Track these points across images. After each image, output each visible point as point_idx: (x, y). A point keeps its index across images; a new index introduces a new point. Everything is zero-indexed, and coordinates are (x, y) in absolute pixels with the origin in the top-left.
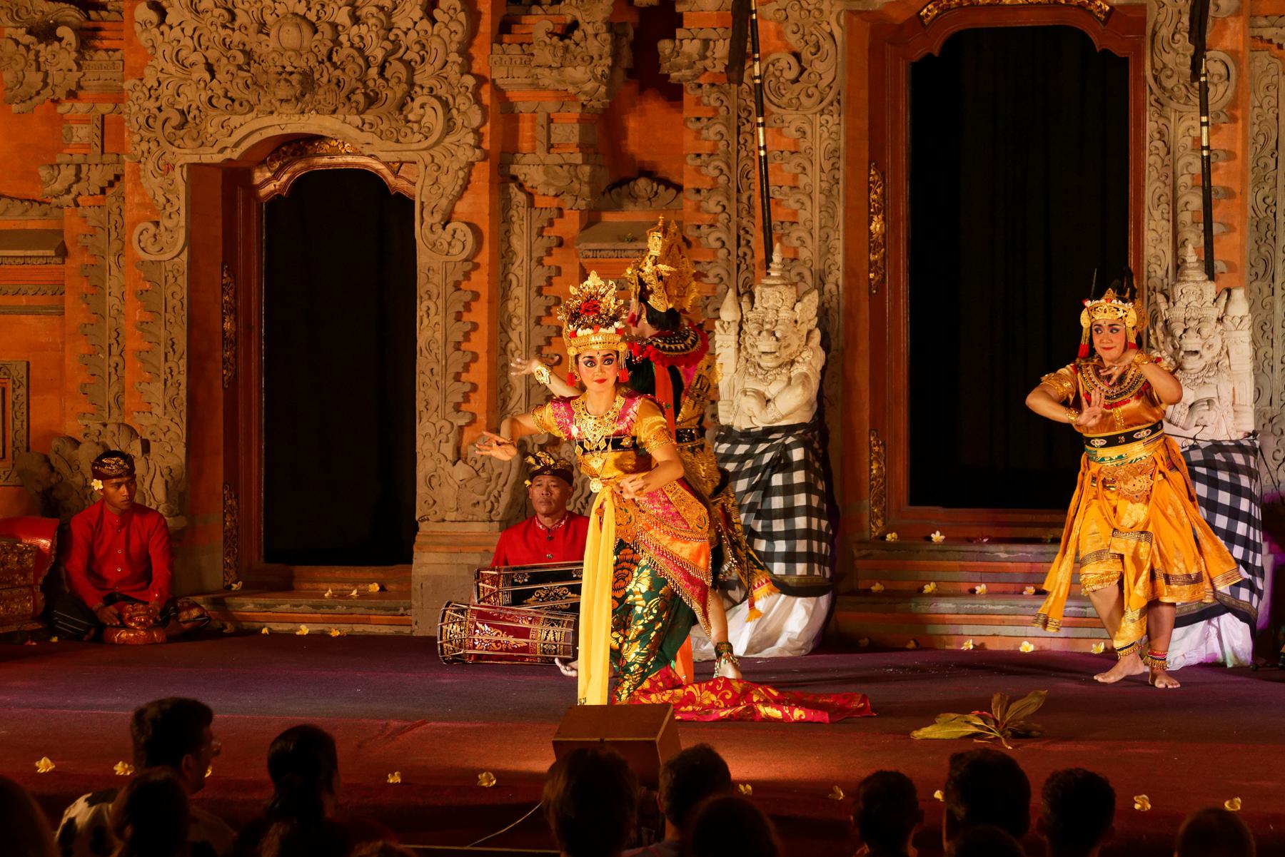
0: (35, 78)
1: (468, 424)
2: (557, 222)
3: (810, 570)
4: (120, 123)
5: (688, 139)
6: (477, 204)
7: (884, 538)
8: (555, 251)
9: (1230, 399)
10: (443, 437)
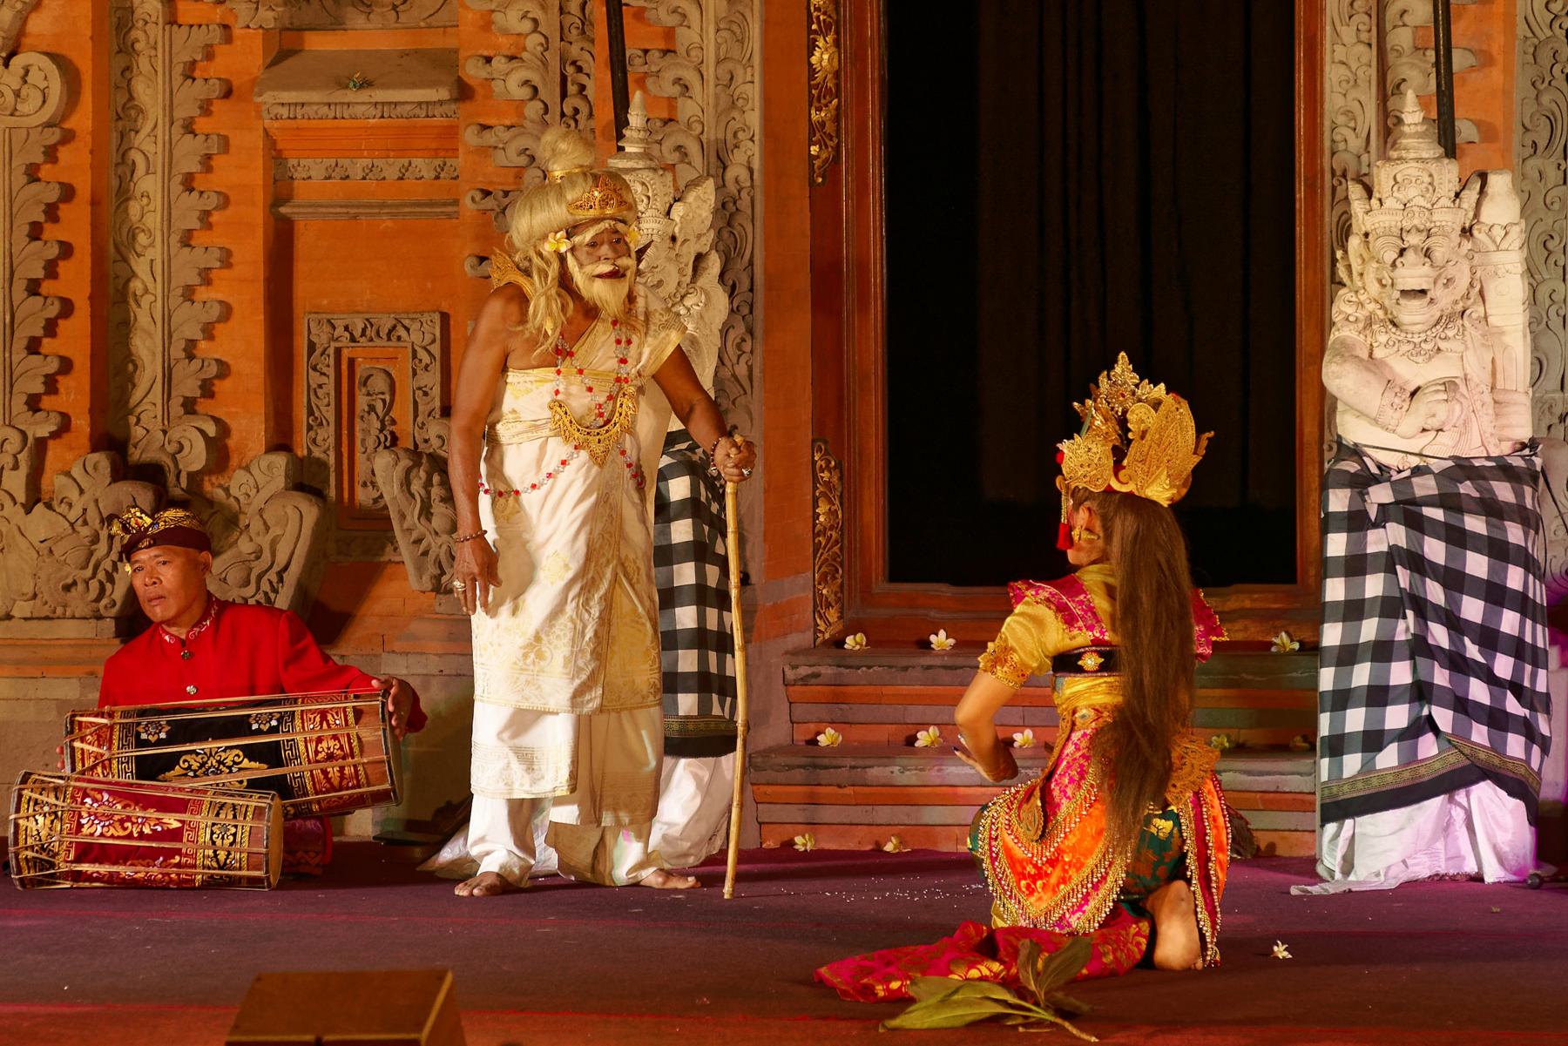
1: (55, 435)
2: (222, 50)
3: (704, 706)
7: (840, 643)
8: (217, 107)
9: (1489, 380)
10: (7, 460)
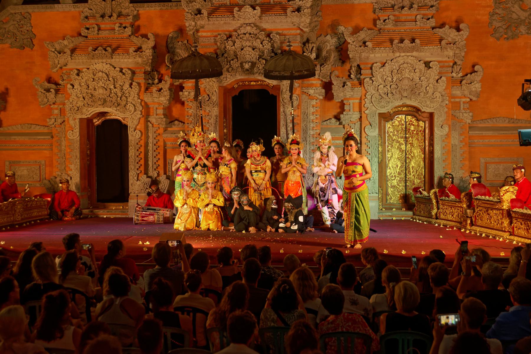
0: (46, 100)
4: (64, 109)
5: (186, 113)
6: (141, 126)
